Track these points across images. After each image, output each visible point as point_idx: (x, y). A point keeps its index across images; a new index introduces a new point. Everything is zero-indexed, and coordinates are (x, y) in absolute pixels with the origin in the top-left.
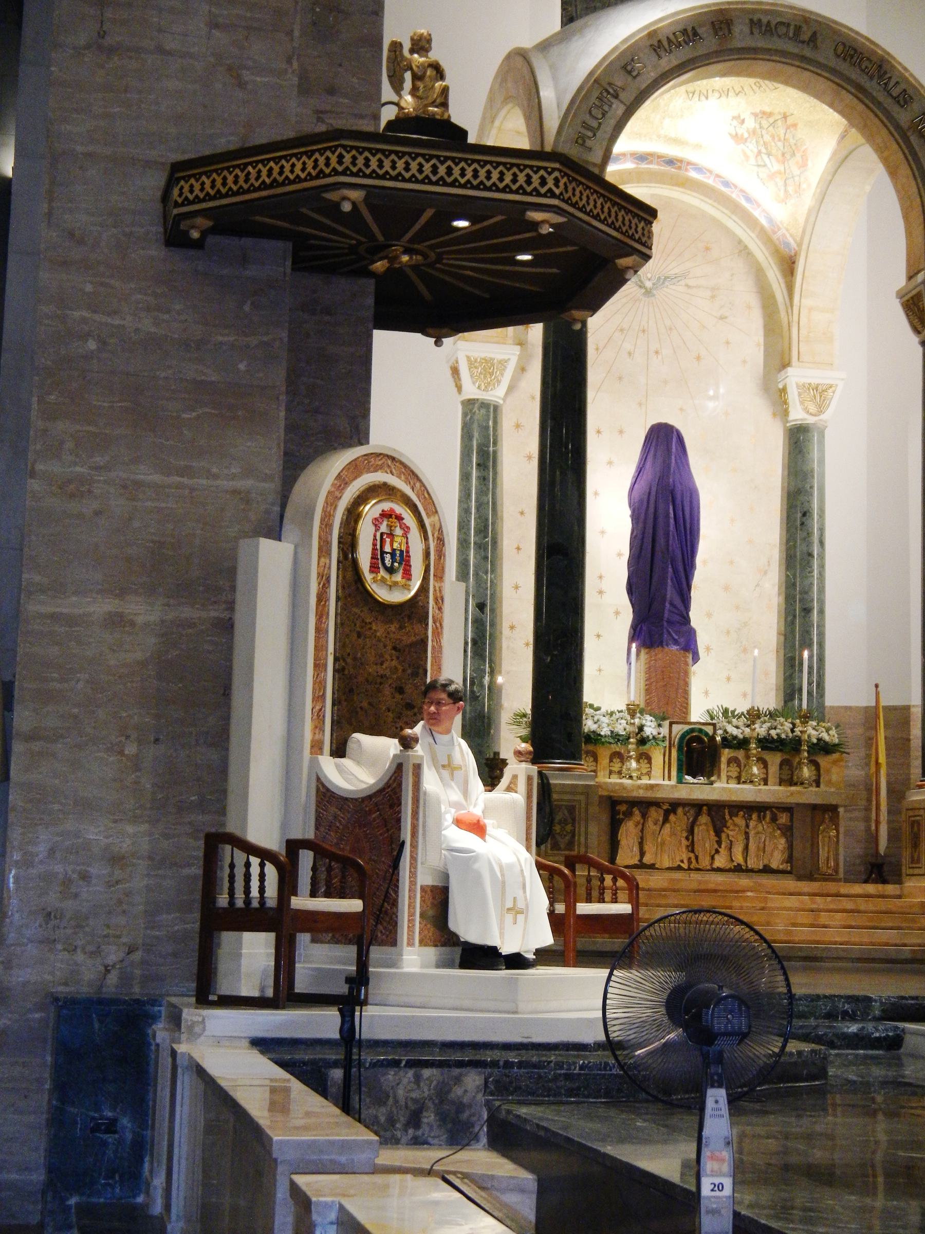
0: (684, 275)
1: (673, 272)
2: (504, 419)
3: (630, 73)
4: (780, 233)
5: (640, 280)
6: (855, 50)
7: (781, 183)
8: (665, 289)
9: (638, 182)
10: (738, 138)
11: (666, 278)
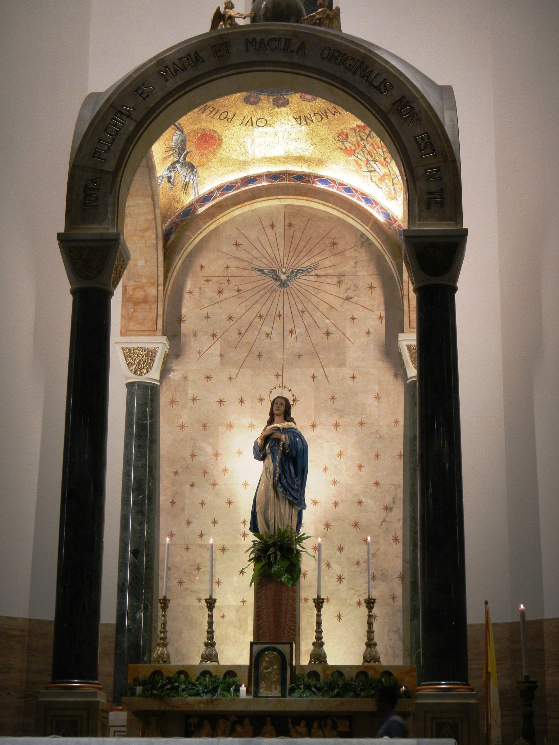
0: (315, 267)
1: (304, 265)
2: (160, 398)
3: (140, 95)
4: (395, 225)
5: (276, 275)
6: (340, 53)
7: (390, 184)
8: (297, 280)
9: (268, 196)
10: (349, 152)
11: (298, 271)
